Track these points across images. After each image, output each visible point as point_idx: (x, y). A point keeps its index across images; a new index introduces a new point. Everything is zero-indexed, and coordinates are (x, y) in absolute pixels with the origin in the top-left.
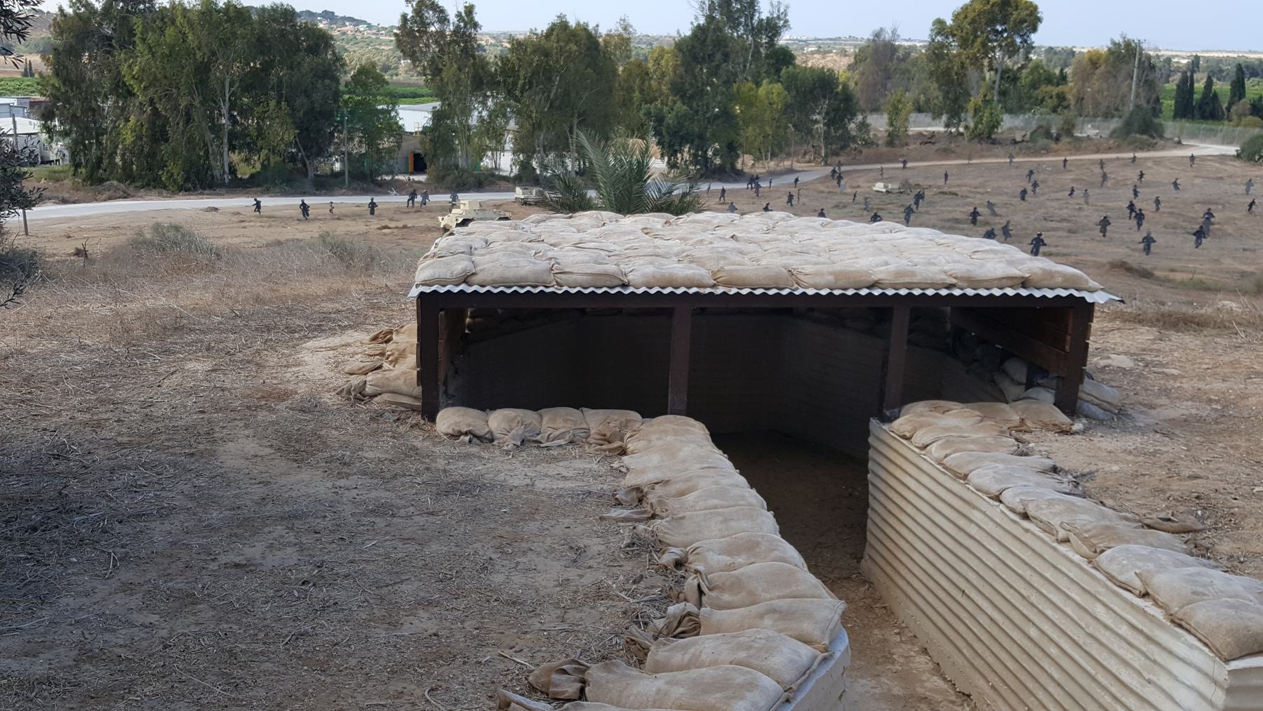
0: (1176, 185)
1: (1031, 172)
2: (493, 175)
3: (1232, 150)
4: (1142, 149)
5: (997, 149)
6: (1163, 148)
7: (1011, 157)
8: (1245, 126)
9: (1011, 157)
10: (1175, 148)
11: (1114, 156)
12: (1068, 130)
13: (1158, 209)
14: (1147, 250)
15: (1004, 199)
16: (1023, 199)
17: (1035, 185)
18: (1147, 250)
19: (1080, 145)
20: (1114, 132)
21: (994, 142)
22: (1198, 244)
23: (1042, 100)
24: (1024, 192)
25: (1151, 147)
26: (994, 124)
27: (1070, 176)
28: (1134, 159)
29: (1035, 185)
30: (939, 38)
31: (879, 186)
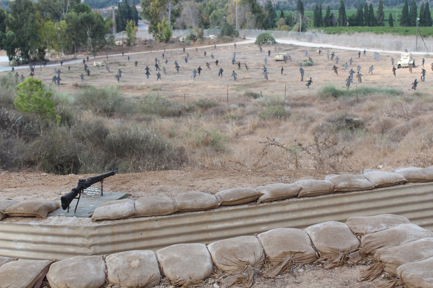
3: (253, 40)
4: (227, 42)
8: (282, 30)
10: (241, 41)
12: (201, 36)
25: (232, 41)
26: (169, 35)
28: (215, 47)
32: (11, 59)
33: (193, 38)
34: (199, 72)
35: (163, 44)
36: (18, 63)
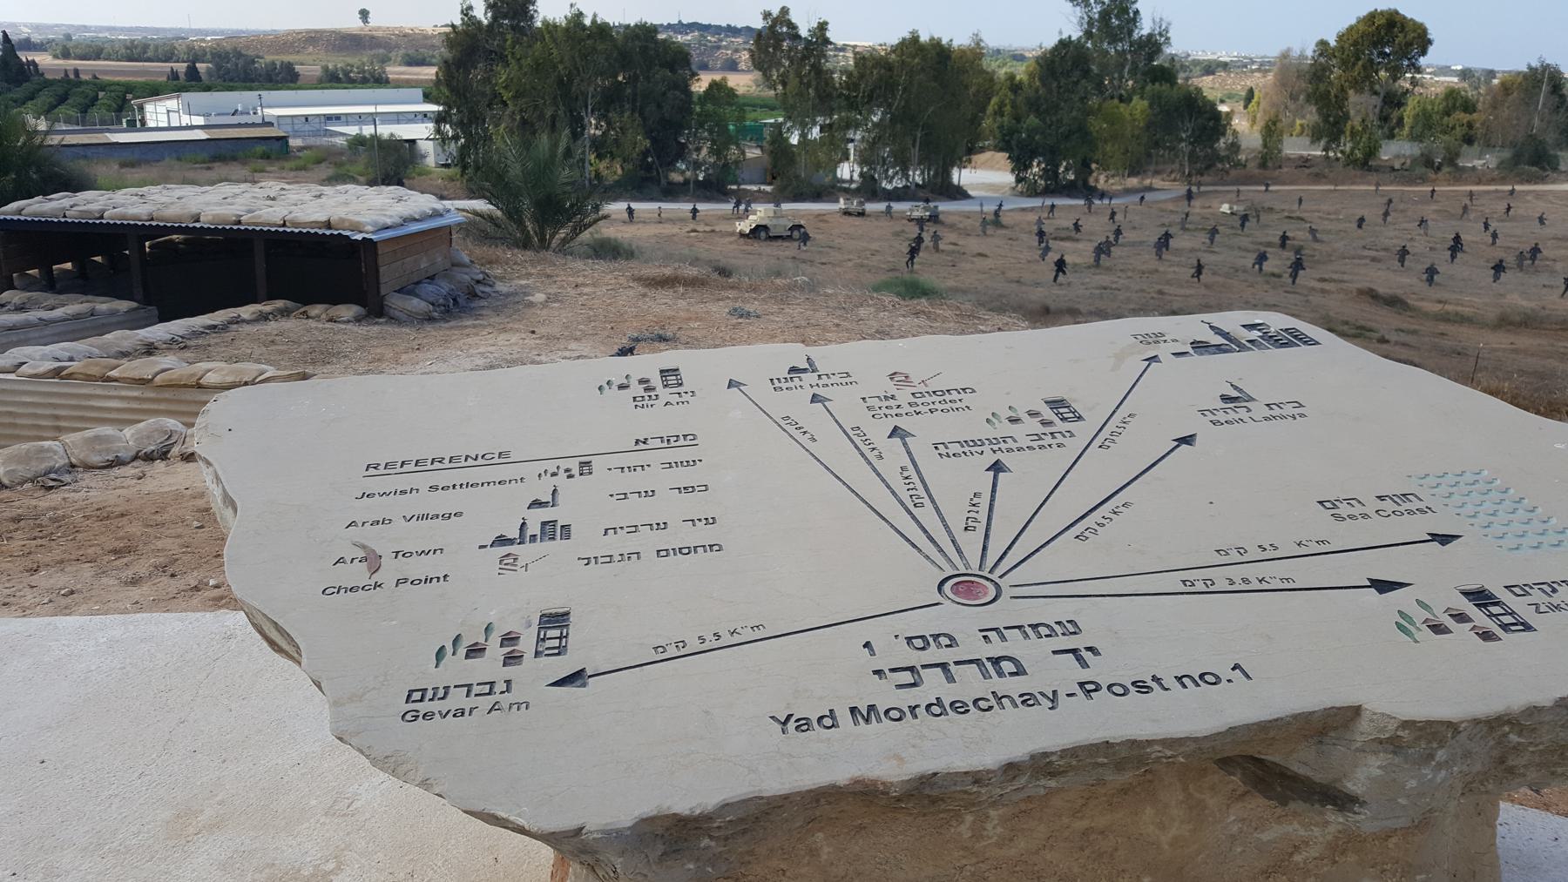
0: (1541, 220)
1: (1390, 201)
2: (833, 187)
4: (1529, 182)
5: (1374, 177)
6: (1553, 182)
7: (1378, 185)
9: (1378, 185)
11: (1492, 188)
12: (1451, 159)
13: (1494, 243)
14: (1430, 281)
15: (1341, 226)
16: (1360, 226)
17: (1386, 214)
18: (1430, 281)
19: (1459, 175)
20: (1502, 162)
21: (1370, 169)
22: (1496, 278)
23: (1453, 128)
24: (1361, 221)
25: (1542, 180)
27: (1434, 207)
29: (1386, 214)
30: (1322, 60)
31: (1225, 208)
32: (1019, 180)
33: (1427, 161)
34: (1533, 258)
35: (1351, 171)
36: (1033, 192)
